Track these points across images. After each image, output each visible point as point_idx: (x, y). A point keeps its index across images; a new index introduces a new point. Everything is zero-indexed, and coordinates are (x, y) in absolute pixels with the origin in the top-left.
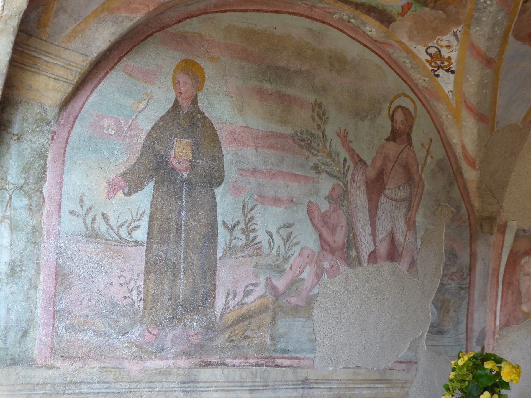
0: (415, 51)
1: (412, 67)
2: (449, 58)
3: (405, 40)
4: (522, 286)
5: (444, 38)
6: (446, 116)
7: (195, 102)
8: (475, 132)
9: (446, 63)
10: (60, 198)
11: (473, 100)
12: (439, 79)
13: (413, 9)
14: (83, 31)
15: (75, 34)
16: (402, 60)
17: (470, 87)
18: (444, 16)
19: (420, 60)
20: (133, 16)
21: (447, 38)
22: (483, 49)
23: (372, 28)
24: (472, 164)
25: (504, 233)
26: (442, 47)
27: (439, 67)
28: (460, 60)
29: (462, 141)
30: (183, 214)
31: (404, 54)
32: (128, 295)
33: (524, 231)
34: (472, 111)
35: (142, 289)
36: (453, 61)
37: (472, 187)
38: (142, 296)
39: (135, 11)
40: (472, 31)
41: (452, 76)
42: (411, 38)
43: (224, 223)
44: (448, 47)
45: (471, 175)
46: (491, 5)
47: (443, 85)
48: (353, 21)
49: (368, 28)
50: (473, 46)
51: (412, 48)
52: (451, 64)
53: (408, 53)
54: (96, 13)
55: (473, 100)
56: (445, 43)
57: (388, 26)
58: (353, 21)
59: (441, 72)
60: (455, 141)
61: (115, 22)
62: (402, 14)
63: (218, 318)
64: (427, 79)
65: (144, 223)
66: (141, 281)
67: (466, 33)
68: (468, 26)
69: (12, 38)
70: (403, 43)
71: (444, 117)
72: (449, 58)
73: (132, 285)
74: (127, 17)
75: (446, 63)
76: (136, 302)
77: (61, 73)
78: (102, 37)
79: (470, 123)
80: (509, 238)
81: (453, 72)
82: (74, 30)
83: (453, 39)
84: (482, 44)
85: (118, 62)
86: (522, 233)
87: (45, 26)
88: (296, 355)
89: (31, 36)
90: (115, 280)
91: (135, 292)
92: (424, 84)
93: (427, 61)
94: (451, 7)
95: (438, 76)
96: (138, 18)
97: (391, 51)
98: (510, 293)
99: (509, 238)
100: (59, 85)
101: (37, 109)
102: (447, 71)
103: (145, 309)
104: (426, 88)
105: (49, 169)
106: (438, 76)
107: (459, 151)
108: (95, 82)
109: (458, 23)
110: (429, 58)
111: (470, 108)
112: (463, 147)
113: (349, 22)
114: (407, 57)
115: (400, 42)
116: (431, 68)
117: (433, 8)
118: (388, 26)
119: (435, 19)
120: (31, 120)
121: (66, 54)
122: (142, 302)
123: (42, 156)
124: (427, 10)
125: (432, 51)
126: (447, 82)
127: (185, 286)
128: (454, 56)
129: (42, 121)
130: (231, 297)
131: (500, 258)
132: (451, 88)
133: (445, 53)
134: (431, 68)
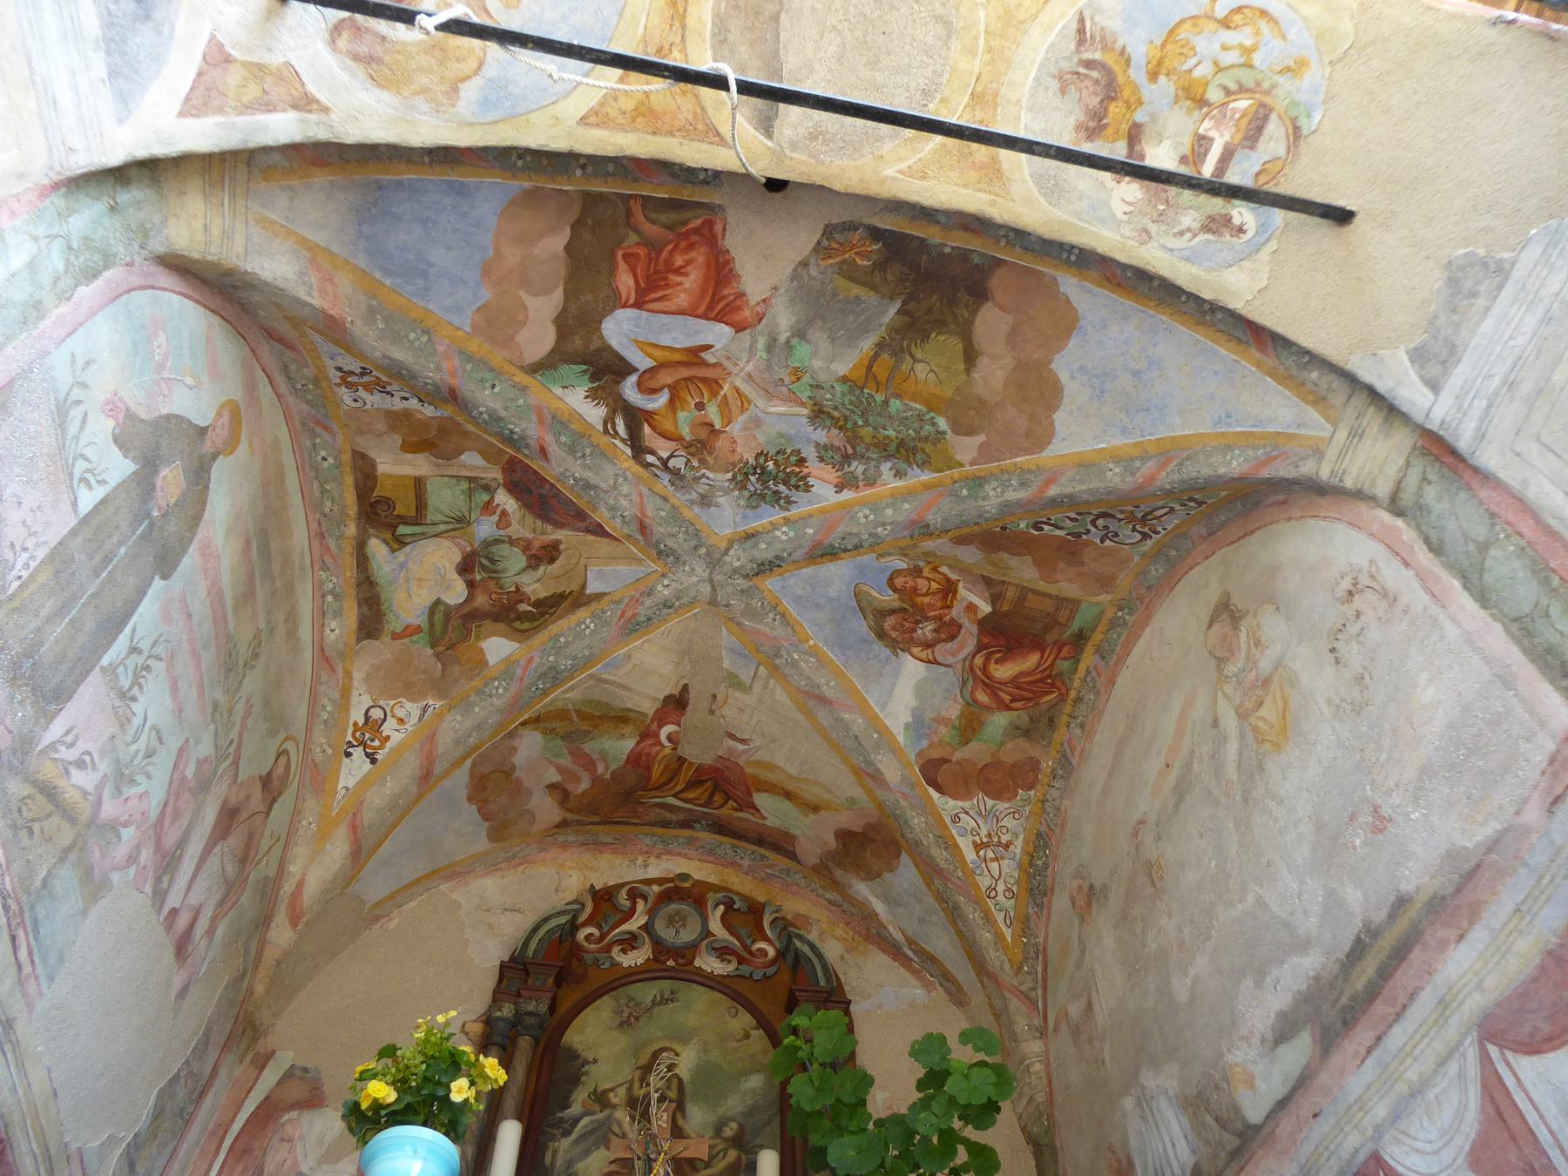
0: (354, 699)
1: (325, 722)
2: (388, 738)
3: (357, 676)
4: (269, 1159)
5: (408, 705)
6: (309, 822)
7: (214, 457)
8: (336, 867)
9: (377, 743)
10: (81, 324)
11: (368, 817)
12: (346, 761)
13: (414, 638)
14: (276, 236)
15: (269, 225)
16: (325, 701)
17: (377, 798)
18: (438, 674)
19: (348, 717)
20: (315, 294)
21: (410, 709)
22: (441, 750)
23: (340, 629)
24: (294, 920)
25: (263, 1068)
26: (393, 716)
27: (363, 743)
28: (399, 749)
29: (304, 874)
30: (123, 551)
31: (336, 695)
32: (18, 548)
33: (306, 1070)
34: (355, 833)
35: (33, 564)
36: (388, 745)
37: (271, 955)
38: (25, 574)
39: (323, 292)
40: (449, 717)
41: (368, 766)
42: (368, 678)
43: (134, 630)
44: (401, 721)
45: (281, 934)
46: (499, 696)
47: (344, 771)
48: (330, 598)
49: (333, 624)
50: (432, 738)
51: (355, 693)
52: (381, 748)
53: (342, 697)
54: (304, 243)
55: (368, 817)
56: (400, 713)
57: (359, 640)
58: (330, 598)
59: (358, 753)
60: (293, 869)
61: (301, 274)
62: (395, 636)
63: (40, 748)
64: (330, 751)
65: (100, 493)
66: (41, 554)
67: (439, 716)
68: (451, 708)
69: (298, 138)
70: (351, 678)
71: (304, 823)
72: (388, 738)
73: (30, 544)
74: (311, 287)
75: (377, 743)
76: (15, 573)
77: (216, 232)
78: (275, 266)
79: (338, 849)
80: (269, 1078)
81: (374, 761)
82: (273, 222)
83: (416, 713)
84: (445, 741)
85: (212, 311)
86: (299, 1073)
87: (266, 180)
88: (37, 960)
89: (249, 165)
90: (26, 505)
91: (25, 556)
92: (319, 757)
93: (355, 724)
94: (457, 668)
95: (348, 755)
96: (313, 302)
97: (324, 677)
98: (240, 1168)
99: (269, 1078)
100: (200, 236)
101: (157, 219)
102: (367, 755)
103: (11, 598)
104: (316, 765)
105: (99, 282)
106: (348, 755)
107: (288, 888)
108: (189, 291)
109: (441, 695)
110: (361, 722)
111: (354, 828)
112: (300, 885)
113: (323, 596)
114: (333, 701)
115: (348, 674)
116: (349, 738)
117: (437, 655)
118: (359, 640)
119: (424, 672)
120: (141, 215)
121: (240, 227)
122: (18, 583)
123: (108, 260)
124: (430, 651)
125: (376, 714)
126: (355, 769)
127: (57, 642)
128: (396, 738)
129: (144, 233)
130: (69, 739)
131: (239, 1108)
132: (351, 784)
133: (387, 729)
134: (349, 738)
